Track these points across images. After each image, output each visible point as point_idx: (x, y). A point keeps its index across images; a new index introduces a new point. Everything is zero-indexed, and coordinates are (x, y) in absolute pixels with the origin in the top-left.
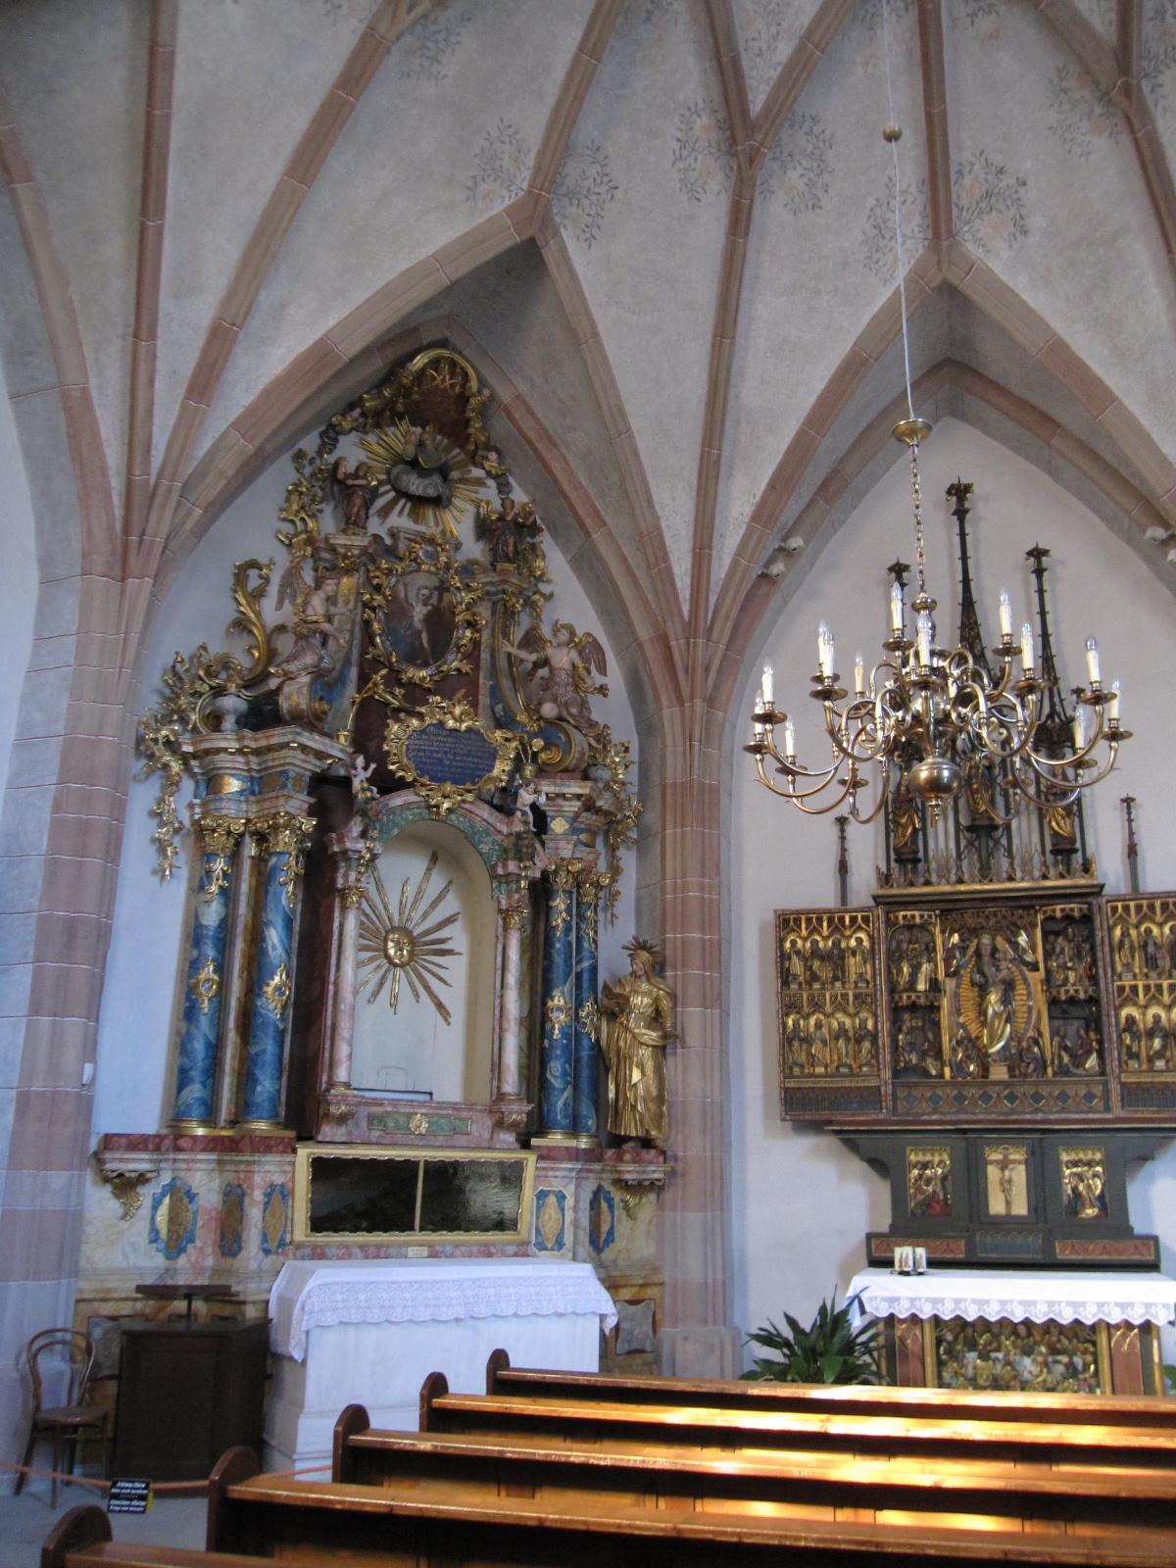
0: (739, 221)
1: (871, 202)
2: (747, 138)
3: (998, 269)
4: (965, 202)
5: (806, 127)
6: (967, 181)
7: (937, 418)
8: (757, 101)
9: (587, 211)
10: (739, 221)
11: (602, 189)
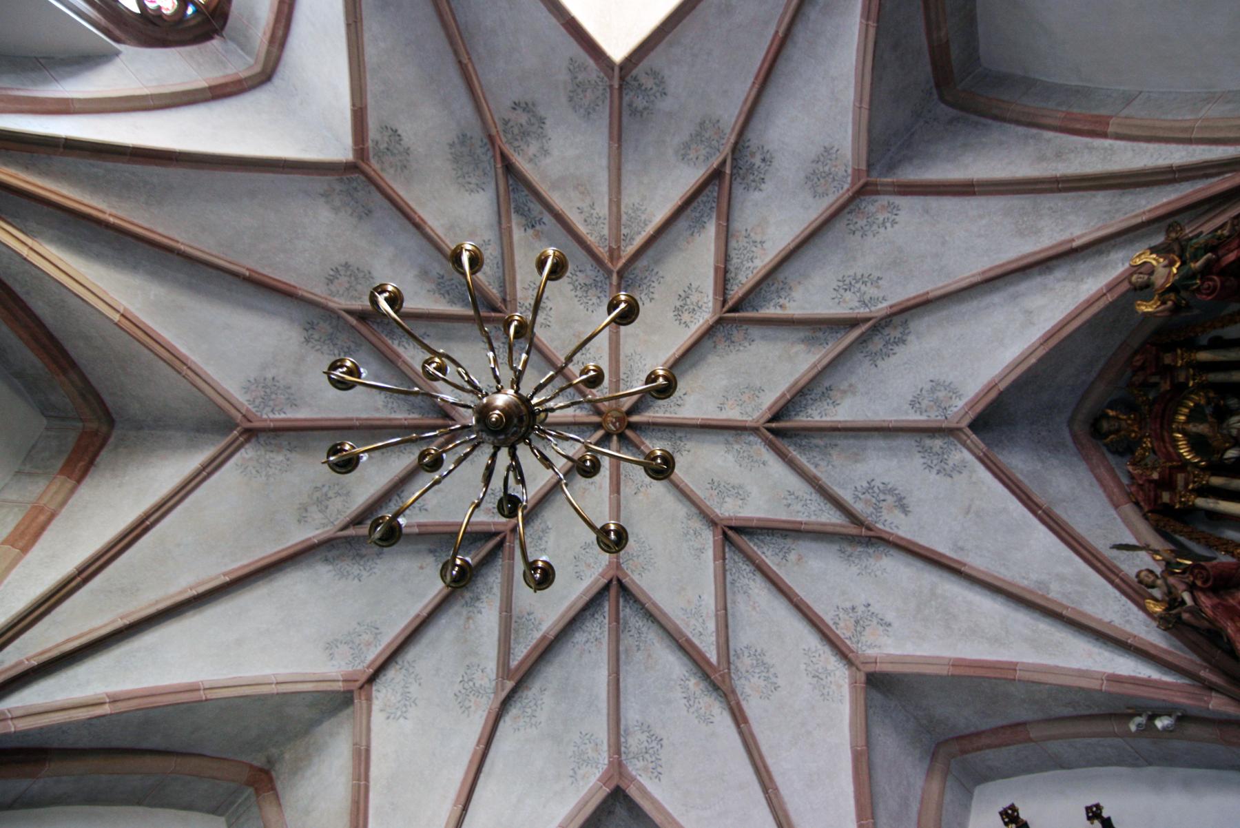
1: (803, 667)
3: (892, 651)
5: (746, 654)
6: (842, 624)
7: (970, 794)
11: (654, 744)
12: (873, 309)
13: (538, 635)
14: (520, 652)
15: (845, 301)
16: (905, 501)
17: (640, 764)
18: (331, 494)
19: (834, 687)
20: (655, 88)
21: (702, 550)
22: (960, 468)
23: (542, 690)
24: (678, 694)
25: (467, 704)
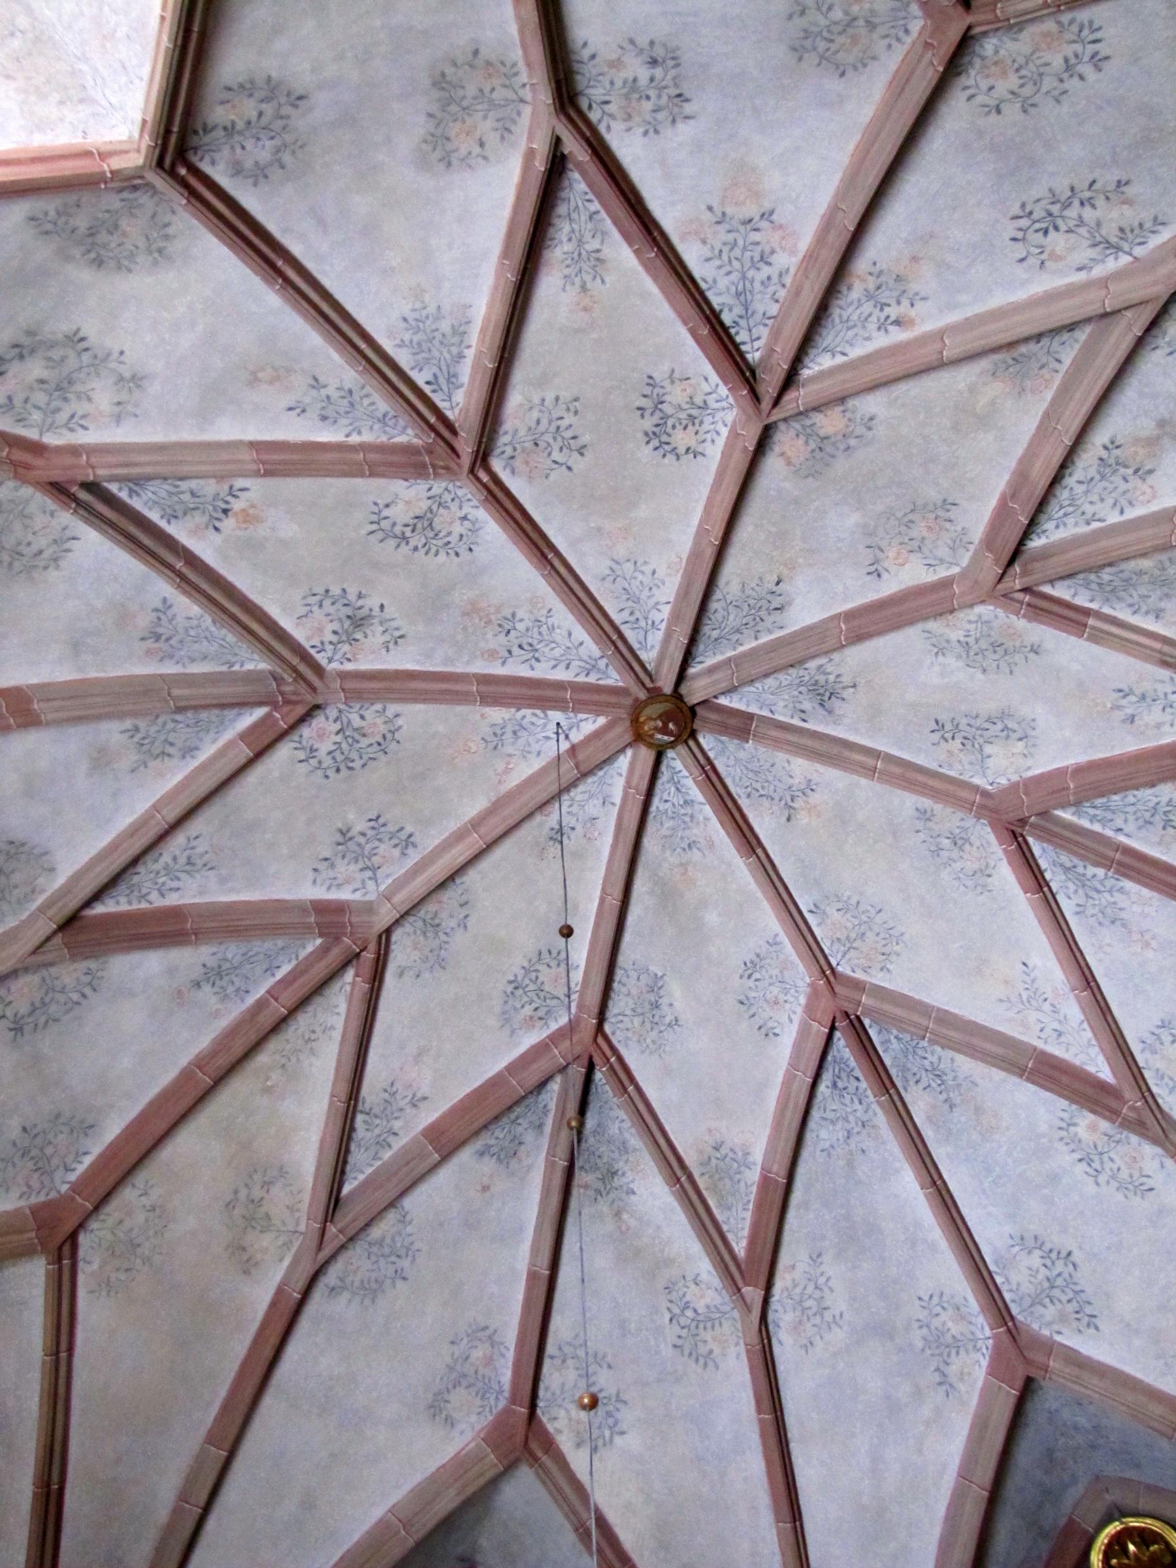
8: (1102, 1069)
9: (1064, 1298)
11: (1059, 1266)
12: (1139, 251)
13: (753, 1176)
15: (1054, 257)
17: (1050, 1312)
18: (257, 1193)
20: (268, 109)
21: (985, 872)
23: (816, 1258)
24: (1065, 1159)
25: (703, 1349)
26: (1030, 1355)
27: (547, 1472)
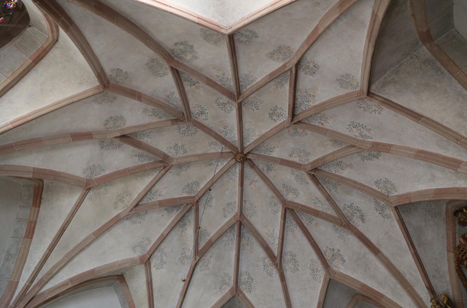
0: (283, 278)
1: (309, 265)
2: (277, 260)
4: (328, 259)
5: (289, 254)
6: (327, 254)
8: (276, 253)
10: (283, 278)
11: (250, 280)
12: (365, 139)
13: (209, 238)
14: (202, 245)
15: (352, 131)
16: (364, 217)
17: (244, 286)
18: (124, 196)
19: (318, 276)
20: (251, 35)
21: (277, 212)
22: (389, 217)
23: (211, 257)
24: (261, 264)
25: (183, 262)
26: (238, 292)
27: (147, 268)
